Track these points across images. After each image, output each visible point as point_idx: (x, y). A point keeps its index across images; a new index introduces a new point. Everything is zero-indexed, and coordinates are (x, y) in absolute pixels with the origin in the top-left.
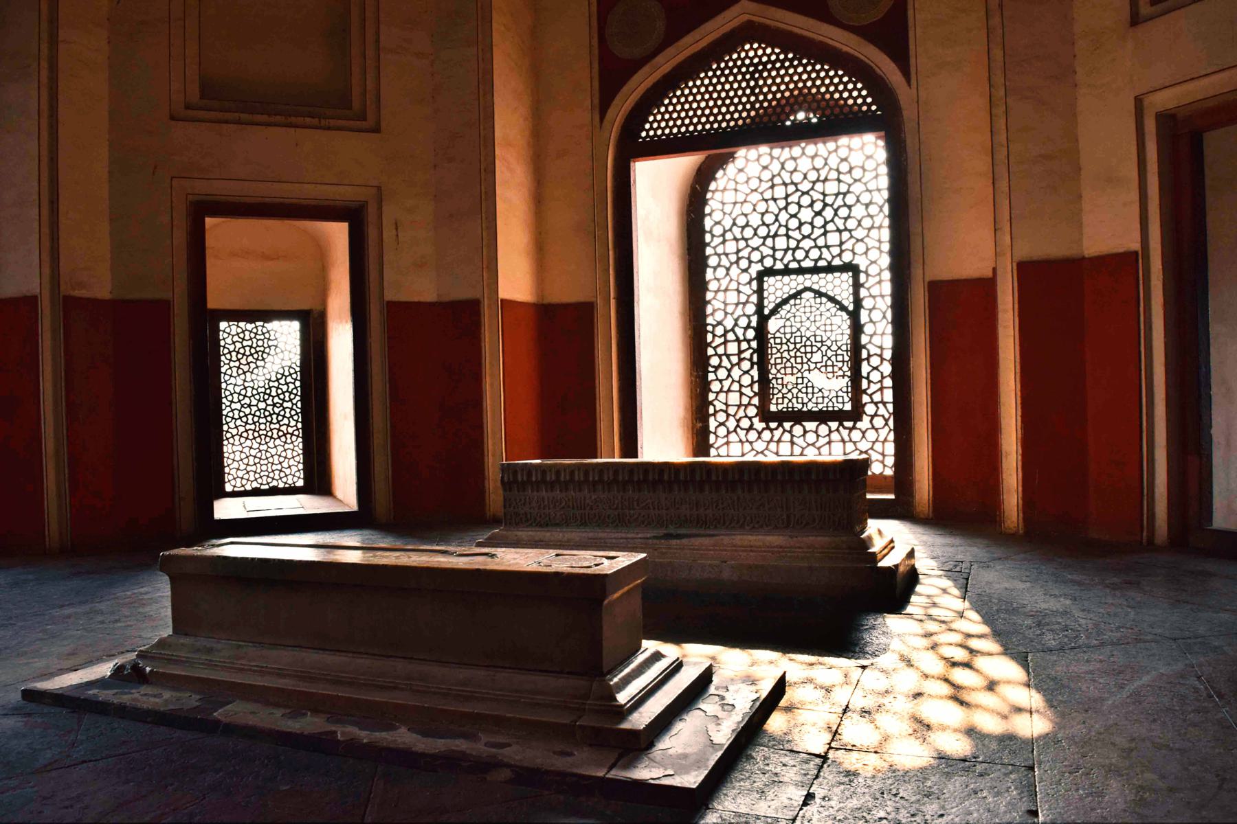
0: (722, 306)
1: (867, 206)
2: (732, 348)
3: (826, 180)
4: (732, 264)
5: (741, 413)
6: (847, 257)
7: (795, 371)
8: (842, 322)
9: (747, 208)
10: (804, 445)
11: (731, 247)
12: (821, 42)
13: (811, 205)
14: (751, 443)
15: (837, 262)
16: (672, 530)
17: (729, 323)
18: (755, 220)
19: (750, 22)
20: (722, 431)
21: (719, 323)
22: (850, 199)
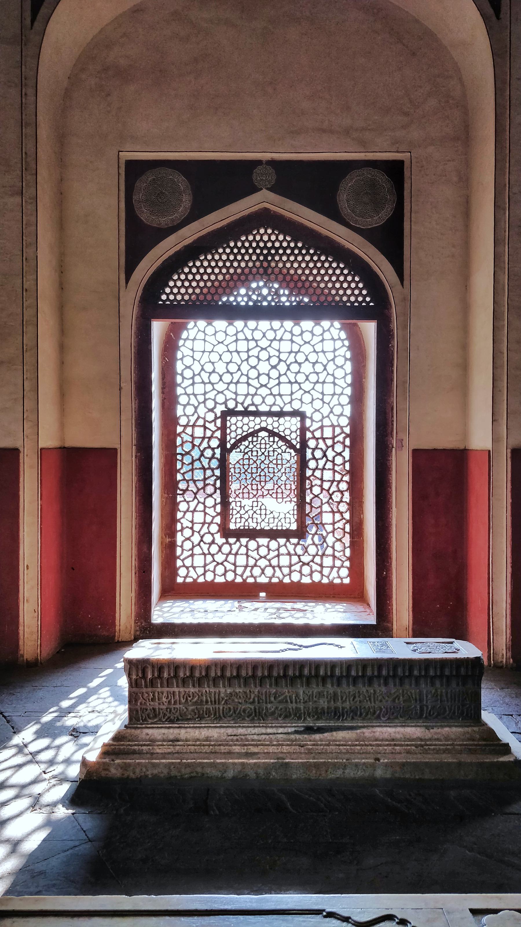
0: (190, 439)
1: (314, 364)
2: (199, 475)
3: (281, 339)
4: (199, 403)
5: (205, 530)
6: (296, 405)
8: (290, 457)
9: (214, 357)
10: (258, 557)
11: (199, 389)
12: (327, 237)
13: (268, 360)
14: (213, 555)
15: (288, 408)
16: (310, 723)
17: (196, 454)
18: (221, 368)
19: (266, 210)
20: (188, 545)
21: (188, 453)
22: (301, 358)
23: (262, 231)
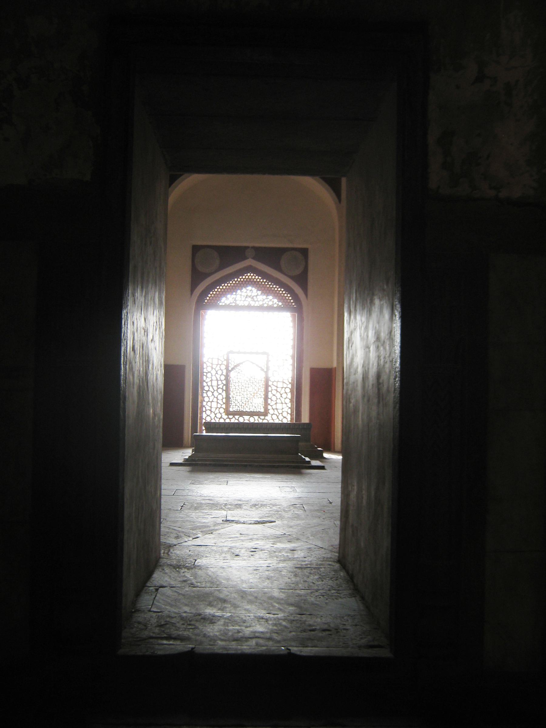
0: (211, 365)
2: (215, 383)
7: (241, 394)
17: (214, 372)
23: (249, 274)
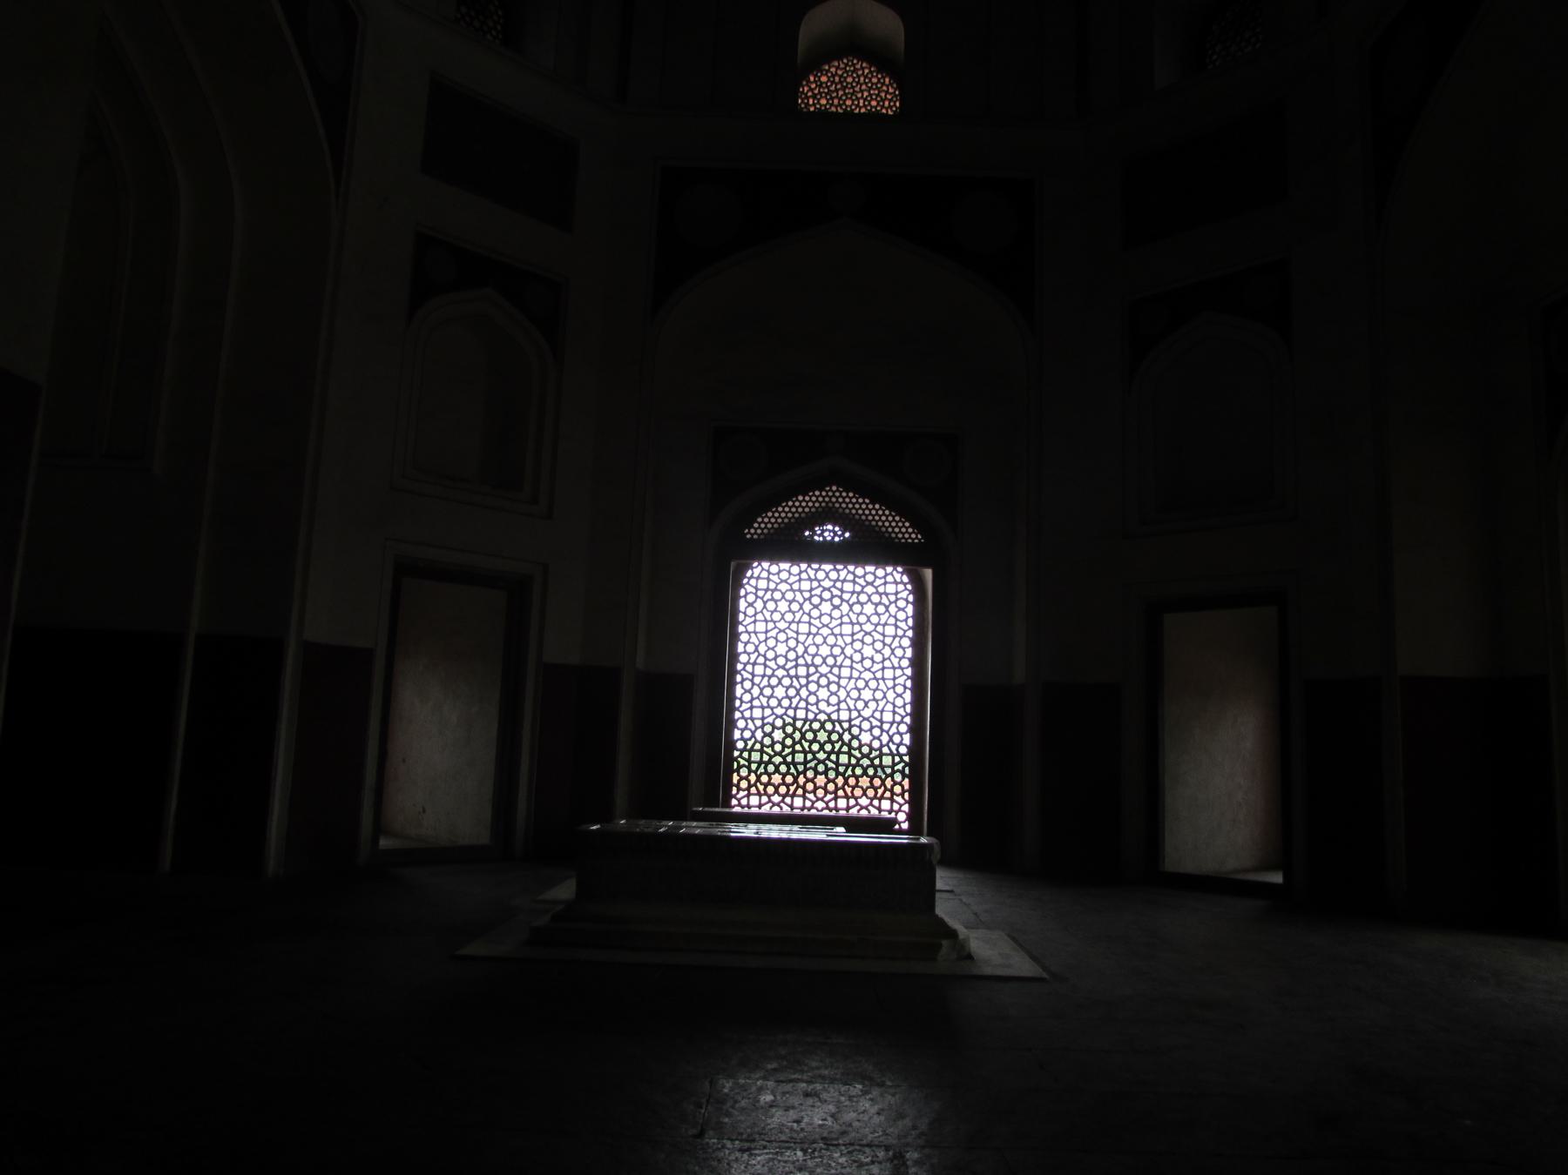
11: (761, 627)
18: (783, 606)
22: (863, 598)
